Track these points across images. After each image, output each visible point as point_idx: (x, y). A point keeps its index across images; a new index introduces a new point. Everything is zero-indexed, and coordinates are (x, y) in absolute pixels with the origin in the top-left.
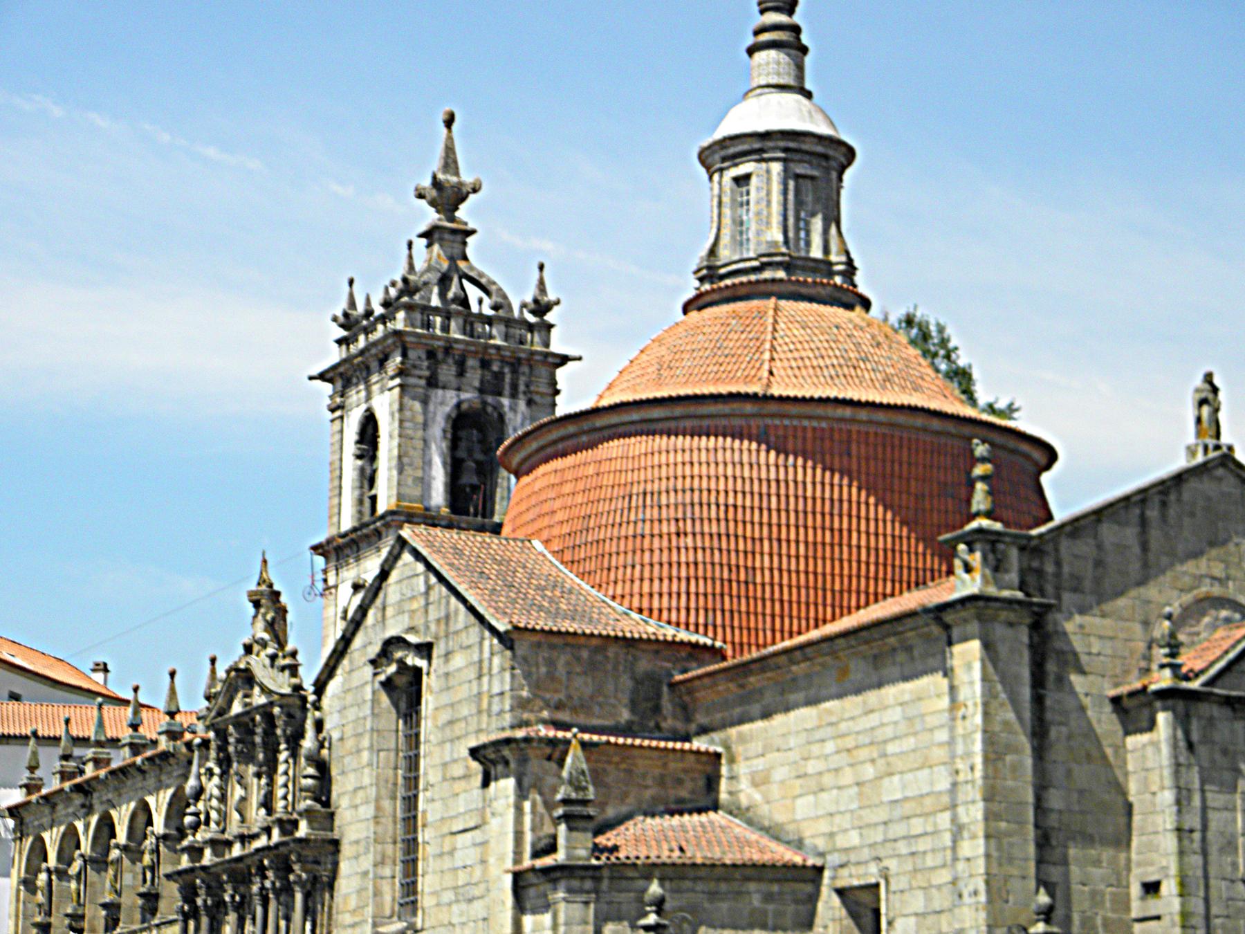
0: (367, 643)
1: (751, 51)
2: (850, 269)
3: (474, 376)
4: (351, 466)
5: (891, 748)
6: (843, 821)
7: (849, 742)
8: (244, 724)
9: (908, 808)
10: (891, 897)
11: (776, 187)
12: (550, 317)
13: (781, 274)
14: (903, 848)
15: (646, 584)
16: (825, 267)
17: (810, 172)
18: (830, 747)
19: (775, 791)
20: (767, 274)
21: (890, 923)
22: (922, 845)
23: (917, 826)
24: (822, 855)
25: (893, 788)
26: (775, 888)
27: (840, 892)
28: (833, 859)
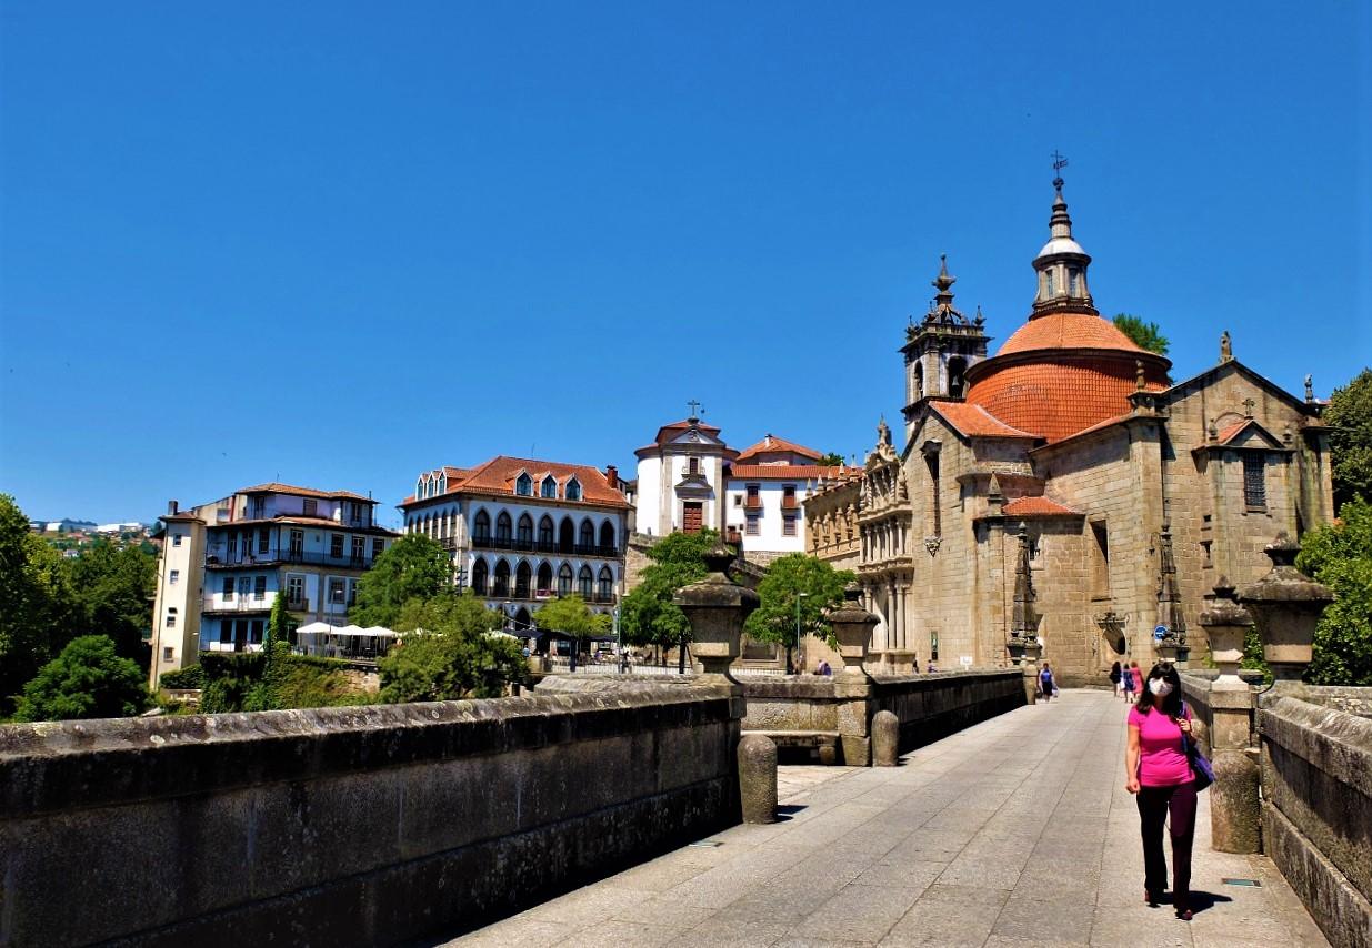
0: (920, 443)
1: (1051, 225)
2: (1091, 301)
3: (956, 347)
4: (913, 381)
5: (1109, 473)
8: (878, 474)
9: (1116, 493)
11: (1061, 273)
12: (982, 325)
13: (1065, 304)
14: (1114, 507)
16: (1081, 300)
19: (1068, 489)
20: (1060, 305)
22: (1122, 506)
23: (1119, 499)
25: (1110, 486)
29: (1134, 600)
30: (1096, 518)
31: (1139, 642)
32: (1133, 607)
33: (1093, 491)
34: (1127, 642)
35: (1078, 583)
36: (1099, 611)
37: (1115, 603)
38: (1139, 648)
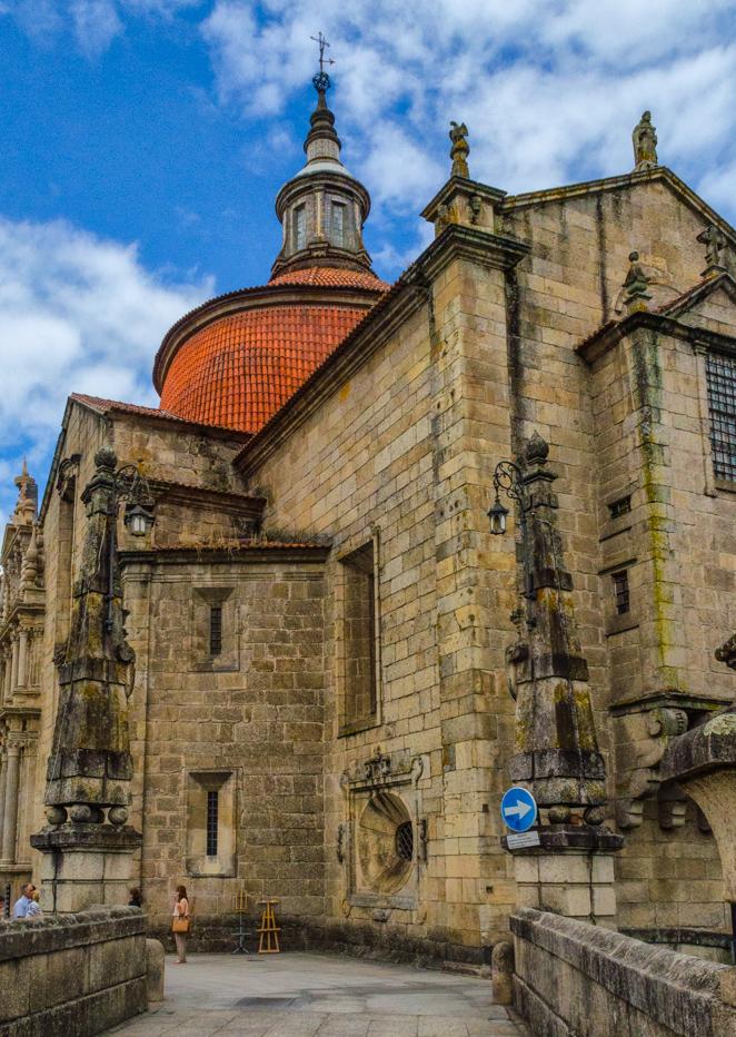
5: (381, 429)
6: (345, 507)
7: (349, 443)
10: (382, 548)
15: (224, 409)
17: (341, 201)
18: (336, 454)
21: (380, 570)
24: (331, 539)
26: (294, 569)
27: (346, 561)
28: (338, 539)
29: (434, 719)
30: (349, 547)
31: (448, 830)
32: (432, 739)
33: (349, 488)
34: (416, 830)
35: (310, 700)
36: (344, 759)
37: (390, 737)
38: (449, 847)
